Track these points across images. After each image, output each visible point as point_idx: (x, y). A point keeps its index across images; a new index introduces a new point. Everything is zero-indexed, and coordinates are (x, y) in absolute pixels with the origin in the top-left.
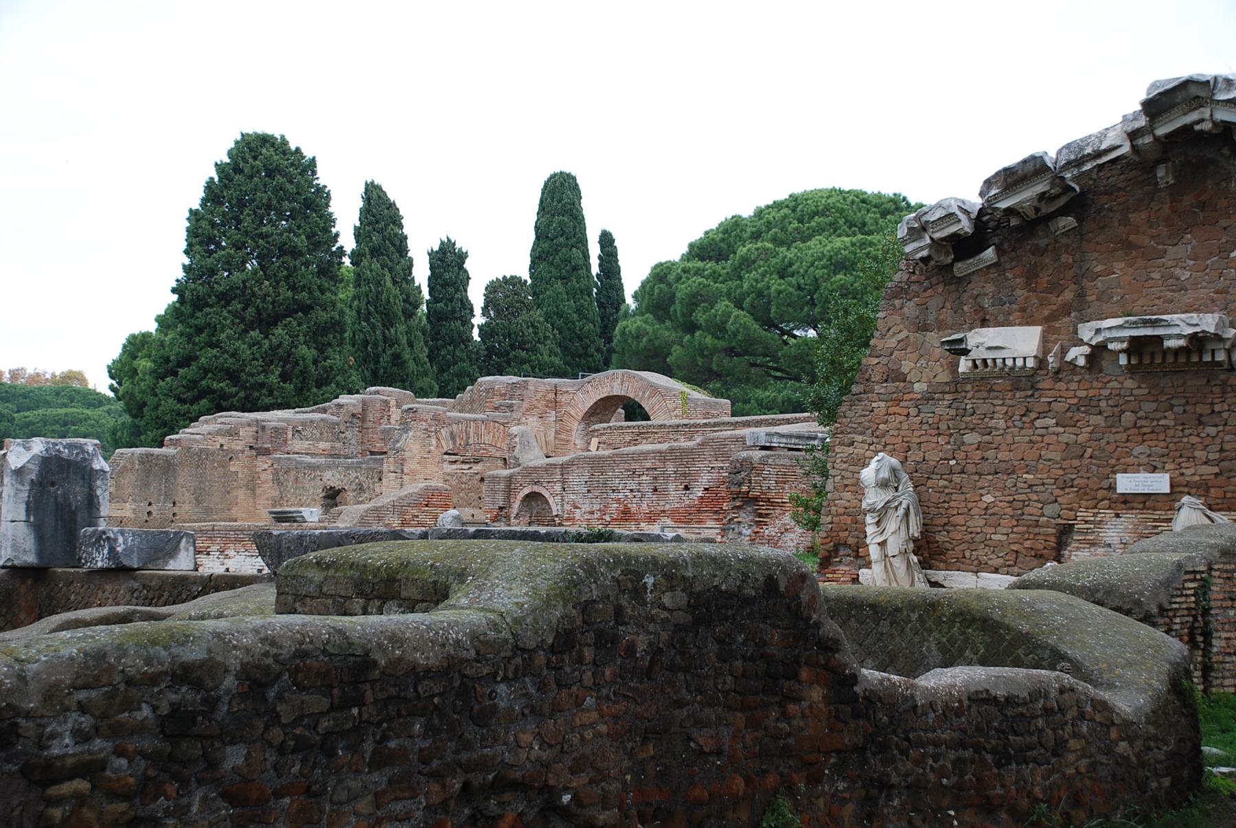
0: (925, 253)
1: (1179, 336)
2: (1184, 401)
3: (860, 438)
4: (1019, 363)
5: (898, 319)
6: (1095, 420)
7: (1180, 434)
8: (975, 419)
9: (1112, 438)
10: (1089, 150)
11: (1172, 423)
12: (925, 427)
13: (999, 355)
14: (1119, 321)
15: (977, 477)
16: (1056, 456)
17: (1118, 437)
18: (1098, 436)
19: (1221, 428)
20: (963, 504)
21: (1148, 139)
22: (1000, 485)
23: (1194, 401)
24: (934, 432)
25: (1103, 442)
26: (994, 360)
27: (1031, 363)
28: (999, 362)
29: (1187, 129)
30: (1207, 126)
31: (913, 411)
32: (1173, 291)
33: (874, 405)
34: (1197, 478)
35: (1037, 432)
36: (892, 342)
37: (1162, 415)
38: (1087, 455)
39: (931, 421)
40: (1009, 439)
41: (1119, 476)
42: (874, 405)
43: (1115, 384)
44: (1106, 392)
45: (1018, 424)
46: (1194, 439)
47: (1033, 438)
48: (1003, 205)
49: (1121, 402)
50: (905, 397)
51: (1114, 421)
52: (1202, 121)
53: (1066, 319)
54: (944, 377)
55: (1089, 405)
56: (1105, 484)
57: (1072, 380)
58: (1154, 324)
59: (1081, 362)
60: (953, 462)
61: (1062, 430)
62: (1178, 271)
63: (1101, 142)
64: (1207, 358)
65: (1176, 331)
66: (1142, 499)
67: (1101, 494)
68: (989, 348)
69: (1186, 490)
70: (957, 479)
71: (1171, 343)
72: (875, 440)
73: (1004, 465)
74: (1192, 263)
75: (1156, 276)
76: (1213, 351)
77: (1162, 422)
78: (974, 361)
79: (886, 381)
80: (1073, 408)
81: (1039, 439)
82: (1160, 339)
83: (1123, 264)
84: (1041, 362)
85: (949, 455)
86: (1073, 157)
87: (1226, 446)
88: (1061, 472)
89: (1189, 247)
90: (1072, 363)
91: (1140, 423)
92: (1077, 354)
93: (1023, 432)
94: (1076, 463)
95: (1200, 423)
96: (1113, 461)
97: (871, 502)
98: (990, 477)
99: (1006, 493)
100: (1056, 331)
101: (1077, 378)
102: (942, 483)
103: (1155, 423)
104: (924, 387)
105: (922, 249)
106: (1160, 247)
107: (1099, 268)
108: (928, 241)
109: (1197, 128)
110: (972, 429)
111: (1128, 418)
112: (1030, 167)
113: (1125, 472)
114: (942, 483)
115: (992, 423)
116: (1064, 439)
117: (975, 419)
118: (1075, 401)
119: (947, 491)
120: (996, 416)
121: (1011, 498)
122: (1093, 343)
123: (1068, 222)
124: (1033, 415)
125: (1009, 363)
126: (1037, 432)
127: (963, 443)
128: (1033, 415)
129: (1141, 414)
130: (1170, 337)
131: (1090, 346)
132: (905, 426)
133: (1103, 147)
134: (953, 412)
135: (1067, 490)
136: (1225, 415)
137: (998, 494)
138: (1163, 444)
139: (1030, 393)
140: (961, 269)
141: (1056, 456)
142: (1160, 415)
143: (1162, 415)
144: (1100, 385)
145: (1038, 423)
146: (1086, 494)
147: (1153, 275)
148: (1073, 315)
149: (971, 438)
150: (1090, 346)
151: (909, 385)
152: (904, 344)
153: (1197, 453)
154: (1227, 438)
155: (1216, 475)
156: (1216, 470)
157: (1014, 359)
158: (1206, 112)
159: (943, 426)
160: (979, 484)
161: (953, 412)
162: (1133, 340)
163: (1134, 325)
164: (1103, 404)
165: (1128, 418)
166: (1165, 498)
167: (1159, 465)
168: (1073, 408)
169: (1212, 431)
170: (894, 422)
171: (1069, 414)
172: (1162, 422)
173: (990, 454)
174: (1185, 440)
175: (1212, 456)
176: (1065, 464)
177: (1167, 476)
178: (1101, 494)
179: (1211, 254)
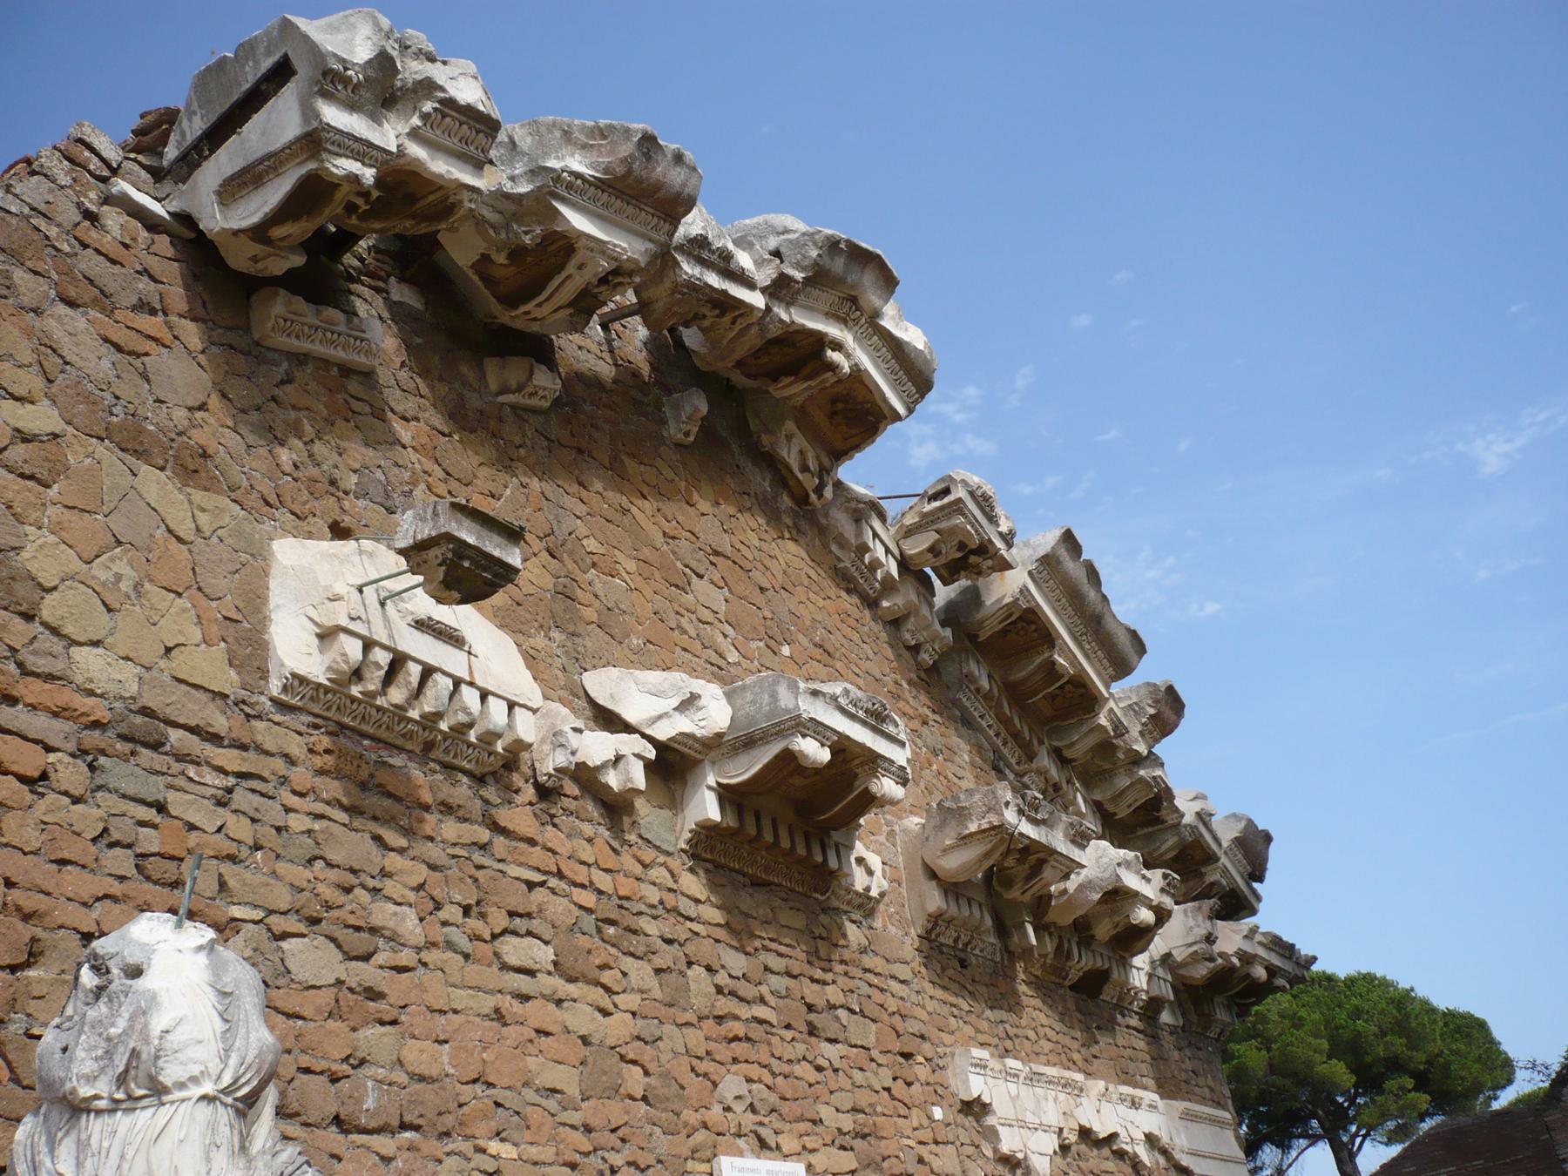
8: (326, 883)
12: (121, 861)
26: (428, 672)
31: (70, 774)
44: (653, 895)
91: (725, 1005)
93: (473, 972)
94: (615, 1111)
95: (812, 1031)
96: (690, 1116)
98: (384, 1144)
110: (315, 921)
115: (382, 913)
120: (390, 887)
122: (663, 732)
128: (499, 920)
129: (722, 978)
151: (48, 642)
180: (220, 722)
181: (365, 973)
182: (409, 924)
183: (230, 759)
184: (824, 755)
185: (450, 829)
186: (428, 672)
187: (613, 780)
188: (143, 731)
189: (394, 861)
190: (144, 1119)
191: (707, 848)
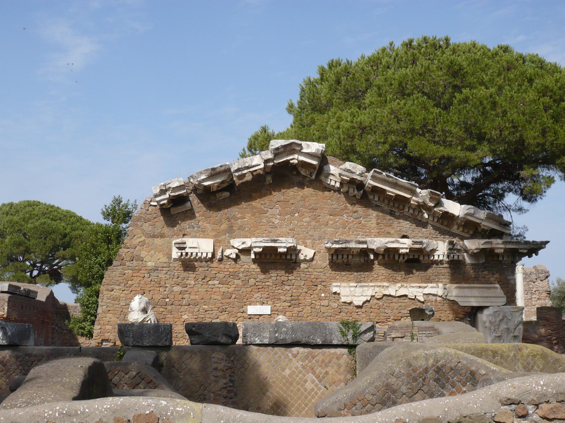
0: (165, 202)
1: (285, 247)
2: (276, 275)
3: (118, 287)
4: (204, 255)
5: (139, 231)
6: (236, 282)
7: (274, 289)
8: (179, 280)
9: (244, 290)
10: (247, 165)
11: (271, 284)
12: (153, 283)
13: (195, 251)
14: (261, 239)
15: (180, 307)
16: (219, 298)
17: (248, 289)
18: (239, 289)
19: (291, 287)
20: (172, 320)
21: (271, 164)
22: (192, 310)
23: (280, 275)
24: (158, 285)
25: (240, 292)
27: (210, 256)
28: (194, 254)
29: (288, 161)
30: (295, 161)
32: (272, 228)
33: (125, 272)
34: (281, 308)
35: (210, 286)
36: (136, 241)
37: (267, 280)
38: (233, 297)
39: (156, 280)
40: (196, 289)
41: (249, 307)
42: (125, 272)
43: (247, 267)
44: (243, 270)
45: (201, 283)
46: (280, 291)
47: (208, 289)
48: (206, 184)
49: (249, 274)
50: (143, 268)
51: (245, 283)
52: (294, 159)
53: (224, 237)
54: (164, 259)
55: (234, 275)
56: (241, 310)
57: (226, 264)
58: (275, 241)
59: (234, 256)
60: (167, 300)
61: (222, 286)
62: (274, 220)
63: (252, 162)
64: (289, 257)
65: (284, 245)
66: (258, 316)
67: (239, 315)
68: (190, 248)
69: (277, 312)
70: (169, 308)
71: (280, 250)
72: (126, 289)
73: (194, 302)
74: (279, 217)
75: (264, 221)
76: (291, 255)
77: (267, 284)
78: (182, 253)
79: (132, 260)
80: (227, 276)
81: (211, 290)
82: (276, 249)
83: (250, 215)
84: (214, 255)
85: (166, 297)
86: (240, 167)
87: (294, 294)
88: (221, 305)
89: (278, 210)
90: (228, 257)
92: (231, 253)
94: (228, 301)
96: (245, 300)
97: (135, 318)
98: (187, 307)
99: (195, 313)
100: (220, 242)
101: (229, 263)
102: (161, 309)
103: (264, 284)
104: (153, 264)
105: (164, 199)
106: (265, 209)
107: (239, 215)
108: (168, 196)
109: (291, 162)
111: (252, 281)
112: (223, 168)
113: (250, 305)
114: (161, 309)
115: (188, 282)
116: (223, 290)
117: (179, 280)
118: (228, 273)
119: (164, 313)
120: (190, 279)
121: (196, 317)
122: (240, 248)
123: (226, 194)
124: (208, 279)
125: (199, 255)
126: (210, 286)
127: (173, 291)
128: (208, 279)
130: (281, 247)
131: (238, 249)
132: (142, 282)
133: (253, 164)
134: (168, 276)
135: (223, 313)
136: (293, 281)
137: (190, 315)
138: (267, 293)
139: (207, 269)
140: (174, 211)
141: (219, 298)
142: (265, 280)
143: (267, 280)
144: (240, 267)
145: (210, 283)
146: (232, 314)
147: (263, 220)
148: (227, 235)
149: (177, 289)
150: (238, 249)
152: (143, 243)
153: (281, 297)
154: (294, 291)
155: (289, 306)
156: (289, 304)
157: (202, 253)
158: (296, 156)
159: (162, 283)
160: (181, 310)
161: (168, 276)
162: (265, 248)
163: (267, 241)
164: (241, 275)
165: (252, 281)
166: (269, 316)
167: (266, 302)
168: (227, 276)
169: (288, 288)
170: (136, 280)
171: (225, 279)
172: (267, 284)
173: (186, 296)
174: (276, 291)
175: (288, 299)
176: (223, 301)
177: (269, 307)
178: (239, 315)
179: (287, 214)
180: (165, 265)
181: (185, 289)
182: (193, 282)
183: (167, 269)
184: (261, 250)
185: (201, 269)
186: (192, 253)
187: (231, 256)
188: (156, 269)
189: (191, 275)
190: (133, 313)
191: (254, 261)
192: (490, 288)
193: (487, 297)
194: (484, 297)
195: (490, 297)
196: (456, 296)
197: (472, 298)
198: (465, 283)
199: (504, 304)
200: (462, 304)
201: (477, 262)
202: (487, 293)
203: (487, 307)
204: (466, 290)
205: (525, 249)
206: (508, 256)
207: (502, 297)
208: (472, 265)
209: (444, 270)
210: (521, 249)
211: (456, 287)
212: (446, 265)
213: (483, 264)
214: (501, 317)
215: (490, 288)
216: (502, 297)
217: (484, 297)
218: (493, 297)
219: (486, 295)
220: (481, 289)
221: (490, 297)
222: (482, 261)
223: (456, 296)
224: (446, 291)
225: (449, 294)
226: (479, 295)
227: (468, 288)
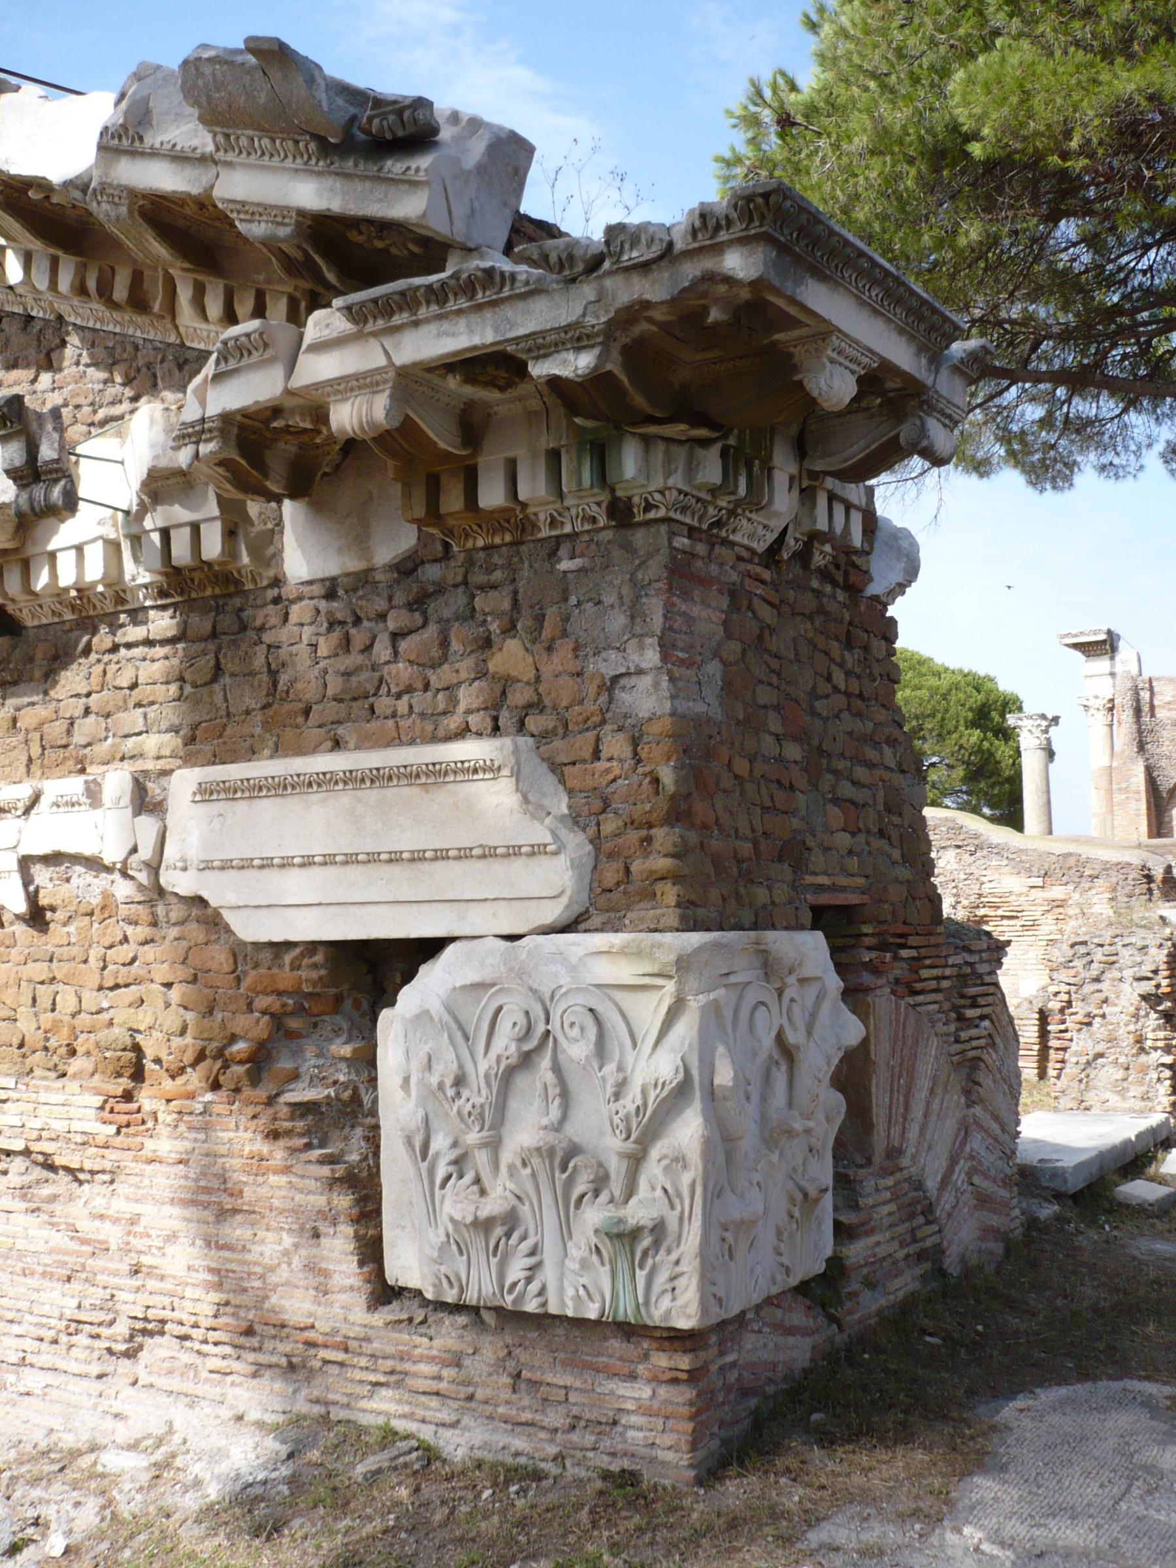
192: (438, 774)
193: (417, 857)
194: (395, 859)
195: (441, 855)
196: (207, 866)
197: (295, 876)
198: (278, 751)
199: (552, 913)
200: (252, 929)
201: (354, 565)
202: (410, 822)
203: (430, 948)
204: (267, 807)
205: (573, 337)
206: (554, 456)
207: (537, 851)
208: (331, 589)
209: (144, 659)
210: (546, 344)
211: (207, 793)
212: (162, 623)
213: (406, 568)
214: (505, 1044)
215: (411, 775)
216: (537, 851)
217: (395, 859)
218: (464, 854)
219: (406, 842)
220: (372, 795)
221: (441, 855)
222: (395, 540)
223: (207, 866)
224: (147, 826)
225: (170, 853)
226: (344, 845)
227: (352, 779)
